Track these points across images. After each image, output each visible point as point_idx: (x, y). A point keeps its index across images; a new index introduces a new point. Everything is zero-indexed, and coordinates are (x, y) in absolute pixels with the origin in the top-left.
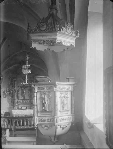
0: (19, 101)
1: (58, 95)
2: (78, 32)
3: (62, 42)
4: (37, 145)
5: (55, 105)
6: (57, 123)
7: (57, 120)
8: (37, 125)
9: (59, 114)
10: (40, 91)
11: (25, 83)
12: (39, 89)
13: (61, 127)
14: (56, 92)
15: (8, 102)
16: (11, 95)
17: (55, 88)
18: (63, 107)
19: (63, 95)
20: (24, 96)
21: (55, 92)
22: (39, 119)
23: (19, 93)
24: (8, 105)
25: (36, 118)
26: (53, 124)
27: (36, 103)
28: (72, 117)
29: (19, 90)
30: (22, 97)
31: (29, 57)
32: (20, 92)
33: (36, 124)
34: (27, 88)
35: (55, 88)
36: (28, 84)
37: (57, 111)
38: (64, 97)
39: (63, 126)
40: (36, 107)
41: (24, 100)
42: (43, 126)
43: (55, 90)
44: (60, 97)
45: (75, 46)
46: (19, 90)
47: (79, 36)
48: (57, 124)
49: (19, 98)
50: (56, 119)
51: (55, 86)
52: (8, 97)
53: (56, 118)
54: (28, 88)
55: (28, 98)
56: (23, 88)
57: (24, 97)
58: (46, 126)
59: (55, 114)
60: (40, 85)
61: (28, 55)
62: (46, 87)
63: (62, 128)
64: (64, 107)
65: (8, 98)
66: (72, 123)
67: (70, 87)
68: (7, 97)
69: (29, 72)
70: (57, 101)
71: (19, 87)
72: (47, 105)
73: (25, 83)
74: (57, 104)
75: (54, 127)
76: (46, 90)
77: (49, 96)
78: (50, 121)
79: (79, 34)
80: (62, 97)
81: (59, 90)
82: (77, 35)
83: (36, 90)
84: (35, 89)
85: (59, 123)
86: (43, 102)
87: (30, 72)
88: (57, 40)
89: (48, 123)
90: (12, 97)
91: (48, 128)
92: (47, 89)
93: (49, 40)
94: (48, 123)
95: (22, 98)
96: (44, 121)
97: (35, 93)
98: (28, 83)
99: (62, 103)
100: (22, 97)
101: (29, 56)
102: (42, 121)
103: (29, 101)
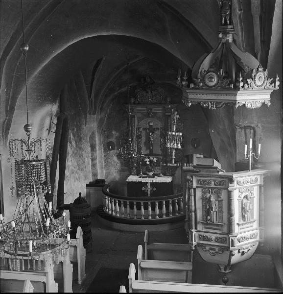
1: (236, 195)
2: (278, 78)
3: (247, 103)
4: (193, 282)
5: (230, 214)
6: (233, 246)
7: (232, 241)
8: (195, 246)
9: (236, 229)
10: (202, 187)
11: (170, 165)
12: (198, 181)
13: (239, 252)
14: (232, 193)
17: (231, 184)
18: (243, 217)
19: (244, 194)
21: (229, 194)
22: (199, 235)
24: (119, 165)
25: (195, 235)
26: (225, 245)
27: (193, 208)
28: (260, 233)
29: (140, 135)
30: (147, 149)
31: (178, 116)
32: (144, 139)
33: (194, 243)
35: (229, 185)
36: (177, 166)
37: (233, 226)
38: (246, 197)
39: (243, 250)
40: (193, 214)
42: (207, 248)
43: (230, 189)
44: (239, 198)
45: (269, 104)
46: (140, 135)
47: (278, 86)
48: (233, 248)
50: (231, 240)
51: (231, 180)
53: (231, 238)
54: (158, 133)
55: (160, 152)
57: (151, 151)
58: (211, 249)
59: (230, 230)
60: (202, 176)
61: (176, 113)
62: (215, 181)
63: (240, 254)
64: (246, 217)
66: (260, 243)
67: (257, 179)
68: (116, 148)
69: (178, 147)
70: (233, 208)
71: (141, 130)
72: (215, 213)
73: (170, 165)
74: (233, 212)
75: (228, 253)
76: (213, 186)
77: (219, 197)
78: (221, 242)
79: (278, 83)
80: (242, 198)
81: (238, 186)
82: (275, 86)
83: (195, 184)
84: (192, 182)
85: (237, 244)
86: (208, 207)
87: (179, 145)
88: (238, 102)
89: (217, 244)
91: (216, 252)
92: (215, 184)
93: (221, 103)
94: (217, 244)
95: (148, 152)
96: (210, 240)
97: (191, 188)
98: (176, 165)
99: (243, 209)
100: (147, 149)
101: (177, 114)
102: (204, 240)
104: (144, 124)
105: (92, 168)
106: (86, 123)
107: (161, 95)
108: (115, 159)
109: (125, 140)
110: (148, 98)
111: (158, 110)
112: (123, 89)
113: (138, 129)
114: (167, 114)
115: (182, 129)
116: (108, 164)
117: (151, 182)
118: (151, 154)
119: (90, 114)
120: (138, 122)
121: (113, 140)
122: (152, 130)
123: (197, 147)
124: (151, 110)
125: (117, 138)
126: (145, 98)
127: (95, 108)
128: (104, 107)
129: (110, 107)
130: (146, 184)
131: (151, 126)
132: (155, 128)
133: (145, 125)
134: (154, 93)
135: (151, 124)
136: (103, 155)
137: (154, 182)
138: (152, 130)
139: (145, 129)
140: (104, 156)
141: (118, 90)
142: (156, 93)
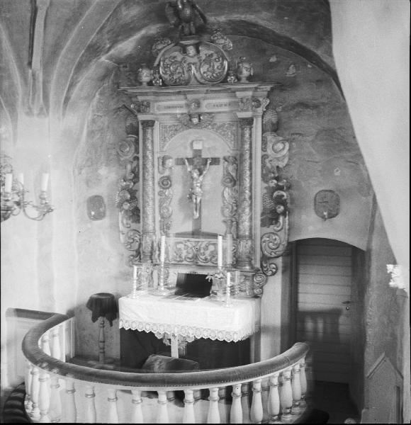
16: (126, 206)
23: (167, 197)
29: (168, 178)
32: (177, 190)
34: (214, 167)
46: (168, 178)
49: (168, 228)
54: (215, 174)
65: (115, 226)
68: (108, 213)
71: (170, 163)
90: (135, 214)
95: (189, 227)
104: (182, 144)
107: (224, 58)
109: (130, 193)
110: (190, 70)
111: (217, 103)
113: (164, 160)
115: (286, 161)
119: (29, 113)
120: (164, 140)
121: (102, 190)
122: (200, 163)
124: (198, 104)
126: (180, 70)
127: (46, 97)
128: (73, 96)
131: (197, 153)
132: (206, 160)
134: (204, 52)
135: (197, 146)
138: (200, 163)
139: (180, 162)
141: (109, 49)
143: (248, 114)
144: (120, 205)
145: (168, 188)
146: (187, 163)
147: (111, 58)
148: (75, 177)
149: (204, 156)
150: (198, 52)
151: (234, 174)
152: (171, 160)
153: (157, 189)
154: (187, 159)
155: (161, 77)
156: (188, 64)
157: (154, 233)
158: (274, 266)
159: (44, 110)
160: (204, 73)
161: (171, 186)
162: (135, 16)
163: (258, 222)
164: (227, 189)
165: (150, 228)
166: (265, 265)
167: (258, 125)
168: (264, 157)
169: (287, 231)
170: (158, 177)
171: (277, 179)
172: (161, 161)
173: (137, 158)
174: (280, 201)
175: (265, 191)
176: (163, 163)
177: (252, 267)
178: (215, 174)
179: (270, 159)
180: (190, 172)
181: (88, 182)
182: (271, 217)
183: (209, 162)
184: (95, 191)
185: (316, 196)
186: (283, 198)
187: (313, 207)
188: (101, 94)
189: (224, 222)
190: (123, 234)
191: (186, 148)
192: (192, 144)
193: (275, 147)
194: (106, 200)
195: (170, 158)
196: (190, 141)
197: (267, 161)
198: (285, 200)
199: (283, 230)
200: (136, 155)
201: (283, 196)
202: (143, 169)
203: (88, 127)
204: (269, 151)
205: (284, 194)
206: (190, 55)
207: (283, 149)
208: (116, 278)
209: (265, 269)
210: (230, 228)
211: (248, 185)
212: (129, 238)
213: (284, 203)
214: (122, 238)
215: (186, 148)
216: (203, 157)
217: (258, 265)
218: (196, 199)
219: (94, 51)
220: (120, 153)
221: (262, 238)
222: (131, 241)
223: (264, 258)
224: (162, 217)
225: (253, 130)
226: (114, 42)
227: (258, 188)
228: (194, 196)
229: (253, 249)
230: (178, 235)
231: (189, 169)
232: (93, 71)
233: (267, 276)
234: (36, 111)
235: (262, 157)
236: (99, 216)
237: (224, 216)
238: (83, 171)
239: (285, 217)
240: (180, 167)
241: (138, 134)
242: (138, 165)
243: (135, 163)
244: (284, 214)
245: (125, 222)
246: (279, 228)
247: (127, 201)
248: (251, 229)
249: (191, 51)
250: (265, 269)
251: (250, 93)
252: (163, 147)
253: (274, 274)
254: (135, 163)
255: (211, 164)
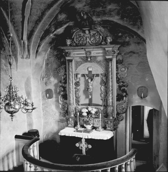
0: (80, 107)
15: (57, 107)
16: (62, 93)
20: (90, 97)
23: (78, 90)
24: (58, 114)
29: (78, 82)
32: (82, 87)
34: (97, 78)
41: (89, 105)
46: (78, 82)
49: (79, 102)
52: (56, 98)
54: (98, 80)
55: (101, 102)
56: (89, 78)
57: (91, 100)
65: (57, 101)
71: (79, 76)
90: (65, 97)
95: (87, 101)
103: (102, 108)
104: (83, 69)
105: (27, 117)
106: (17, 68)
107: (100, 35)
108: (53, 107)
110: (86, 39)
111: (97, 52)
112: (58, 30)
113: (76, 75)
114: (107, 57)
115: (126, 75)
116: (46, 113)
117: (86, 138)
118: (90, 104)
119: (23, 58)
120: (76, 67)
121: (52, 87)
122: (91, 76)
123: (144, 97)
124: (90, 53)
125: (56, 85)
126: (82, 39)
127: (29, 51)
129: (48, 52)
130: (79, 140)
133: (84, 70)
134: (92, 32)
135: (90, 69)
136: (41, 103)
137: (90, 138)
138: (91, 76)
139: (83, 75)
140: (43, 104)
141: (54, 31)
142: (94, 33)
143: (110, 57)
144: (59, 93)
145: (79, 86)
146: (86, 76)
147: (55, 35)
148: (41, 81)
149: (93, 73)
150: (90, 33)
151: (105, 81)
152: (79, 75)
153: (74, 86)
154: (86, 74)
155: (75, 42)
156: (86, 37)
157: (73, 104)
158: (122, 117)
159: (28, 57)
160: (92, 41)
161: (79, 85)
162: (64, 18)
163: (115, 100)
164: (102, 86)
165: (72, 102)
166: (118, 116)
167: (114, 61)
168: (117, 74)
169: (127, 103)
170: (74, 82)
171: (123, 82)
172: (75, 75)
173: (66, 74)
174: (124, 91)
175: (118, 87)
176: (76, 76)
177: (113, 118)
178: (98, 80)
179: (120, 74)
180: (87, 80)
181: (46, 83)
182: (120, 98)
183: (95, 76)
184: (48, 87)
185: (138, 89)
186: (125, 90)
187: (137, 93)
188: (50, 49)
189: (102, 99)
190: (61, 104)
191: (85, 70)
192: (88, 69)
193: (122, 70)
194: (53, 91)
195: (79, 74)
196: (87, 67)
197: (118, 75)
198: (126, 91)
199: (125, 103)
200: (65, 73)
201: (125, 89)
202: (68, 79)
203: (46, 62)
204: (119, 71)
205: (126, 88)
206: (87, 31)
207: (125, 70)
208: (58, 122)
209: (119, 118)
210: (104, 102)
211: (111, 85)
212: (63, 106)
213: (126, 92)
214: (60, 106)
215: (85, 70)
216: (92, 74)
217: (115, 117)
218: (90, 91)
219: (47, 32)
220: (59, 72)
221: (117, 106)
222: (64, 107)
223: (118, 114)
224: (76, 97)
225: (113, 63)
226: (56, 28)
227: (114, 85)
228: (89, 90)
229: (113, 110)
230: (82, 105)
231: (87, 79)
232: (48, 39)
233: (119, 121)
234: (25, 57)
235: (117, 73)
236: (50, 97)
237: (101, 97)
238: (44, 79)
239: (126, 97)
240: (83, 78)
241: (66, 65)
242: (66, 77)
243: (65, 76)
244: (126, 96)
245: (61, 99)
246: (124, 102)
247: (62, 91)
248: (112, 102)
249: (87, 32)
250: (119, 118)
251: (111, 49)
252: (76, 70)
253: (122, 120)
254: (65, 76)
255: (96, 76)
